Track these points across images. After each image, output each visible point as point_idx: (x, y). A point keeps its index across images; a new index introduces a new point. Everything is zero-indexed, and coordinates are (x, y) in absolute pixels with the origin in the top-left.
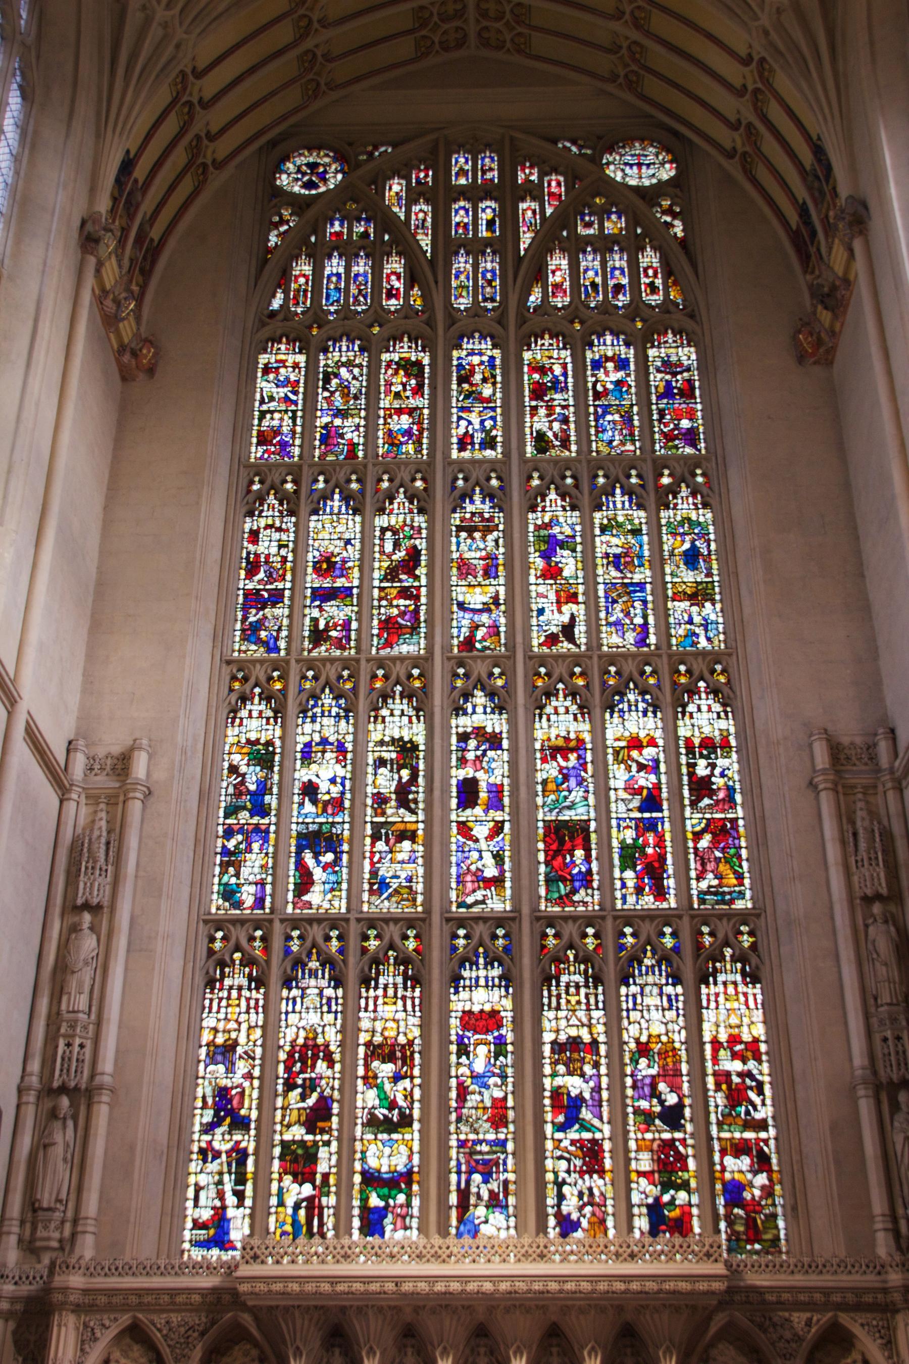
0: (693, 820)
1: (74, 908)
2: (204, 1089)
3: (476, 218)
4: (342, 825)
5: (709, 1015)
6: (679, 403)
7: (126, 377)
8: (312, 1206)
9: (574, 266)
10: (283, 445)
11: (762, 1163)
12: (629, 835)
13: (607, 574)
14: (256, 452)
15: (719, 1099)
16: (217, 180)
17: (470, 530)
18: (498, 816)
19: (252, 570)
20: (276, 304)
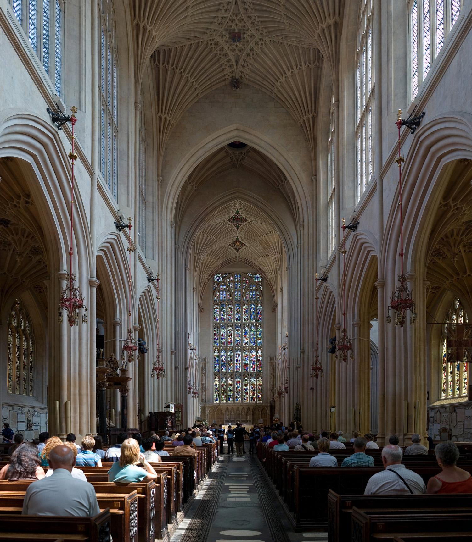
0: (258, 363)
3: (238, 286)
9: (249, 293)
17: (237, 331)
20: (215, 299)
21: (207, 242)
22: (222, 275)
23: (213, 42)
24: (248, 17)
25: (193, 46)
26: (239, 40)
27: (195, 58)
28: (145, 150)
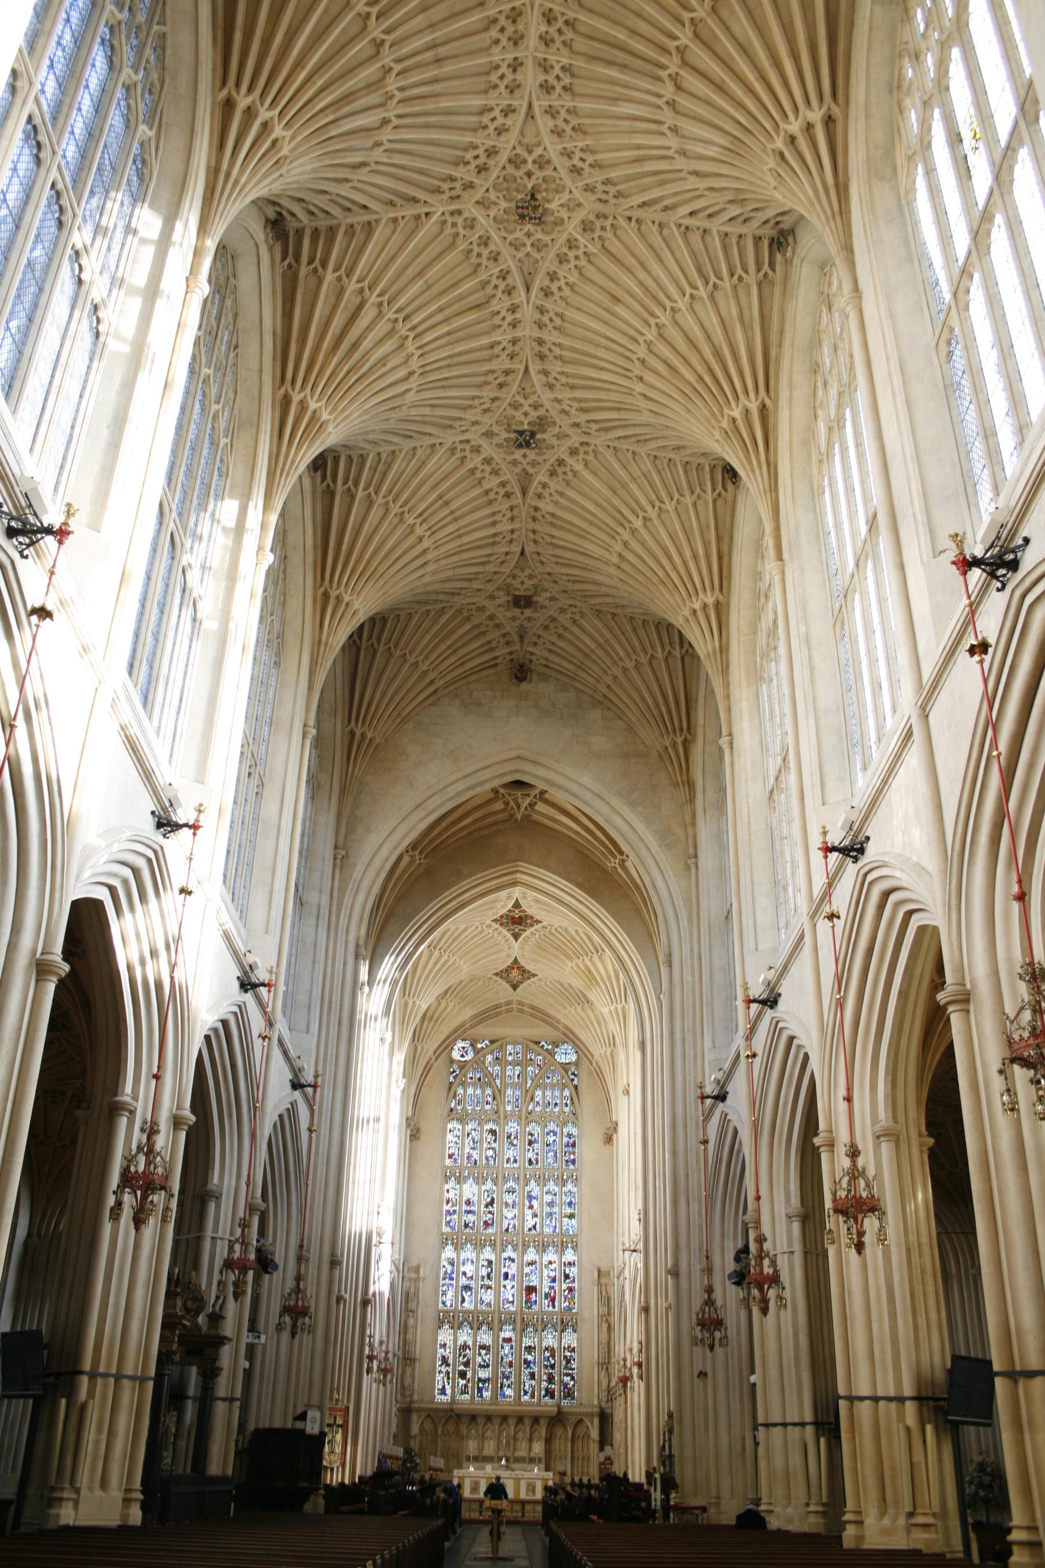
0: (564, 1286)
1: (407, 1310)
2: (439, 1356)
4: (473, 1284)
5: (563, 1341)
6: (570, 1149)
7: (411, 1140)
8: (466, 1386)
9: (544, 1094)
10: (455, 1160)
11: (573, 1378)
12: (547, 1290)
13: (547, 1209)
14: (448, 1162)
15: (564, 1362)
16: (435, 1065)
18: (514, 1283)
19: (448, 1202)
20: (453, 1105)
21: (438, 967)
22: (472, 1045)
28: (313, 798)
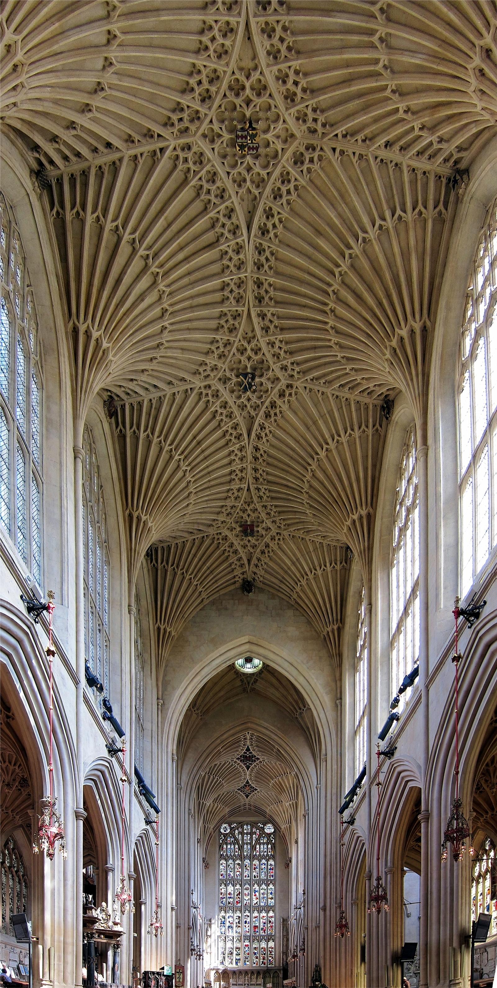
13: (262, 896)
23: (220, 537)
24: (263, 506)
25: (197, 541)
26: (252, 534)
27: (198, 556)
